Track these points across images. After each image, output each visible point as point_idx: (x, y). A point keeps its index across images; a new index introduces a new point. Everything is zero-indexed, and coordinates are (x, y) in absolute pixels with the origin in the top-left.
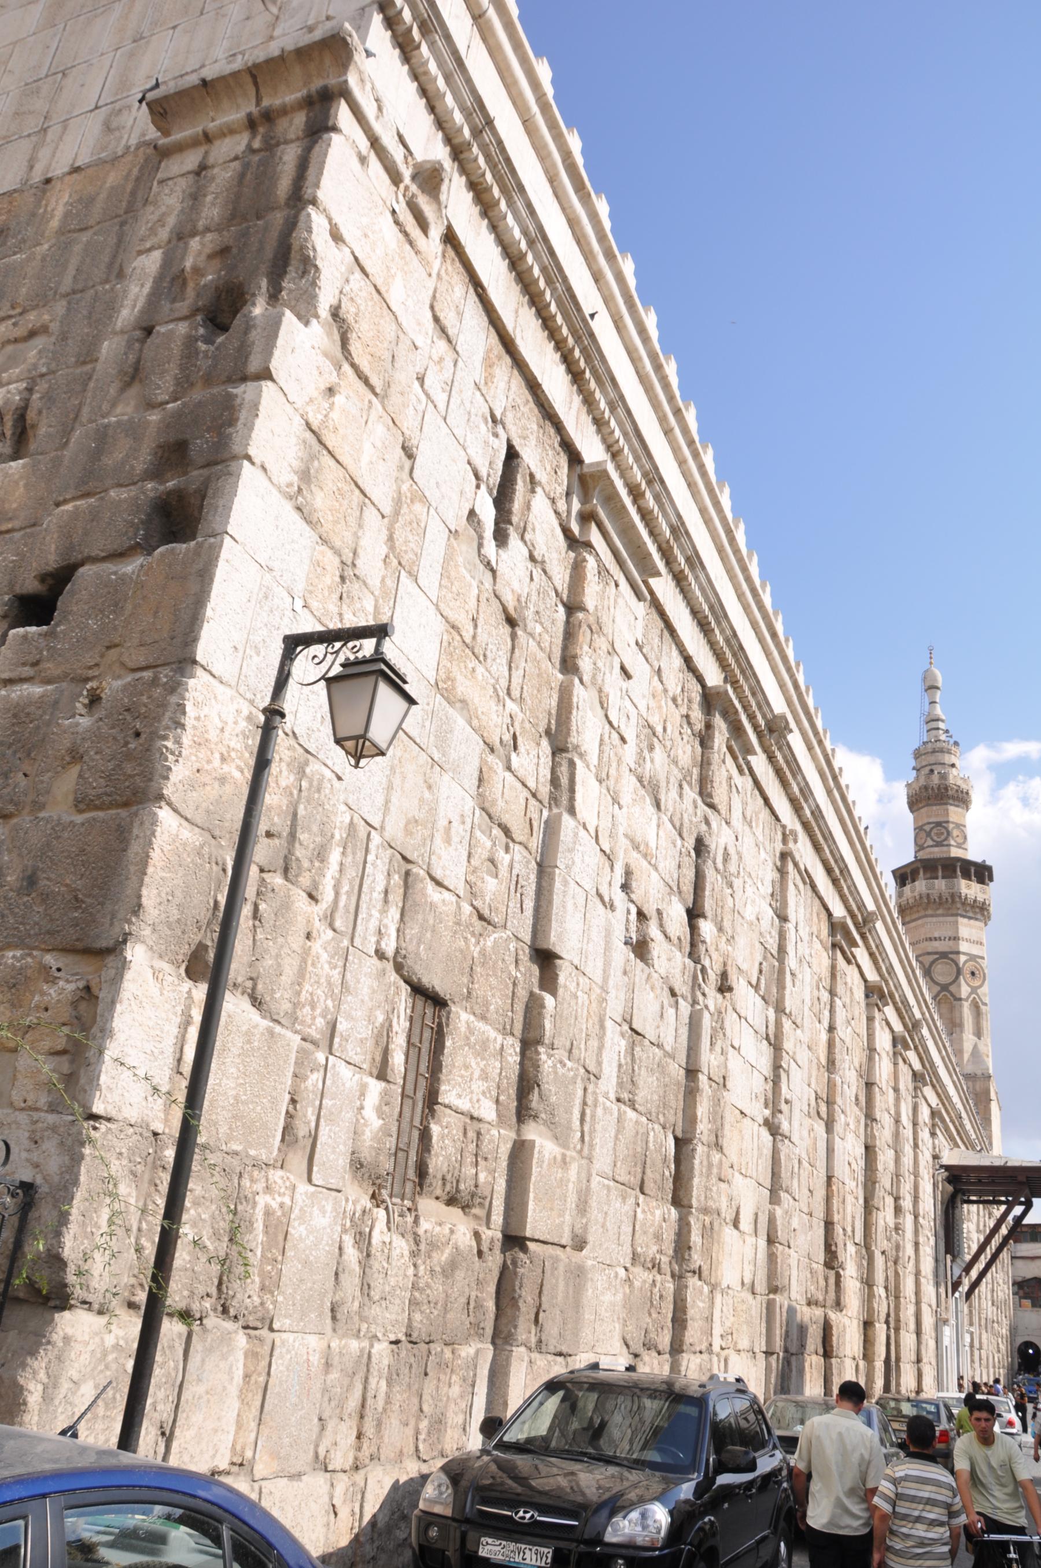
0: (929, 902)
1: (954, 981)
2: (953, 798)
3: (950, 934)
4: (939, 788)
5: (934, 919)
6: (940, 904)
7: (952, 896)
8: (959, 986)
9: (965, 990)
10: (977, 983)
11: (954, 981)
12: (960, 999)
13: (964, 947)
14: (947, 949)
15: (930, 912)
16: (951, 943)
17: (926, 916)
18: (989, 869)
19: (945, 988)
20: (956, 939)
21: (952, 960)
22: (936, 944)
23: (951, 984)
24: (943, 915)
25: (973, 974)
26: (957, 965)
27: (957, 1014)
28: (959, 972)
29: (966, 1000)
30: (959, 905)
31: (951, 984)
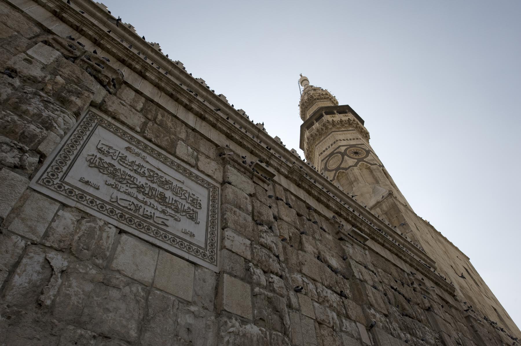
0: (314, 139)
2: (318, 99)
4: (308, 99)
5: (321, 144)
6: (321, 134)
7: (324, 125)
8: (346, 161)
10: (360, 157)
14: (333, 150)
15: (317, 143)
17: (316, 146)
18: (347, 107)
21: (337, 153)
22: (324, 154)
23: (341, 164)
24: (324, 138)
27: (351, 176)
29: (356, 165)
30: (330, 127)
31: (341, 164)
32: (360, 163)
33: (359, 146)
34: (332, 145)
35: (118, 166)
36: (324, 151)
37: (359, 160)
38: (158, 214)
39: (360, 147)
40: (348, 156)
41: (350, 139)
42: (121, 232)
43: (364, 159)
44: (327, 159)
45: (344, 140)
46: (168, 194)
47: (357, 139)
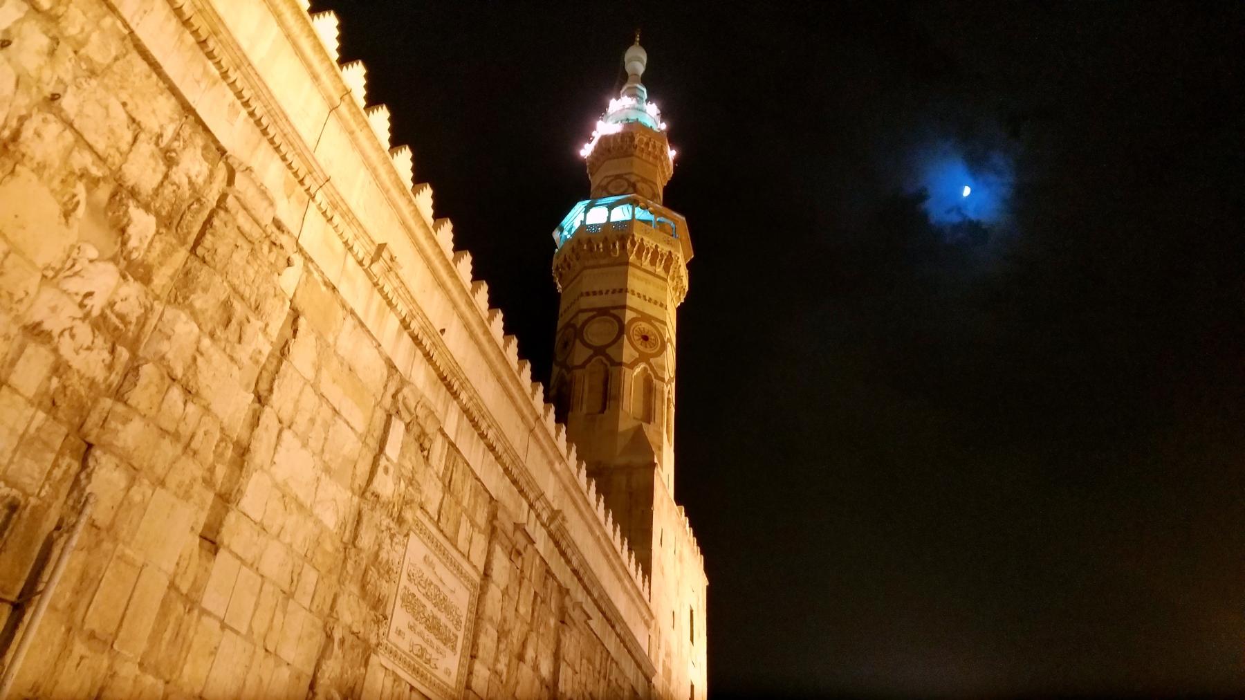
1: (614, 342)
3: (617, 286)
5: (596, 271)
8: (621, 347)
9: (628, 353)
10: (648, 351)
11: (614, 342)
12: (621, 364)
13: (631, 301)
16: (616, 296)
19: (600, 351)
20: (623, 291)
21: (615, 316)
23: (608, 346)
25: (645, 338)
26: (620, 321)
28: (622, 330)
31: (608, 346)
32: (642, 366)
33: (657, 324)
34: (614, 292)
35: (418, 595)
36: (594, 293)
37: (644, 358)
38: (435, 655)
39: (656, 328)
40: (629, 339)
41: (650, 300)
42: (412, 688)
43: (652, 360)
44: (591, 314)
45: (639, 296)
46: (443, 618)
47: (661, 305)
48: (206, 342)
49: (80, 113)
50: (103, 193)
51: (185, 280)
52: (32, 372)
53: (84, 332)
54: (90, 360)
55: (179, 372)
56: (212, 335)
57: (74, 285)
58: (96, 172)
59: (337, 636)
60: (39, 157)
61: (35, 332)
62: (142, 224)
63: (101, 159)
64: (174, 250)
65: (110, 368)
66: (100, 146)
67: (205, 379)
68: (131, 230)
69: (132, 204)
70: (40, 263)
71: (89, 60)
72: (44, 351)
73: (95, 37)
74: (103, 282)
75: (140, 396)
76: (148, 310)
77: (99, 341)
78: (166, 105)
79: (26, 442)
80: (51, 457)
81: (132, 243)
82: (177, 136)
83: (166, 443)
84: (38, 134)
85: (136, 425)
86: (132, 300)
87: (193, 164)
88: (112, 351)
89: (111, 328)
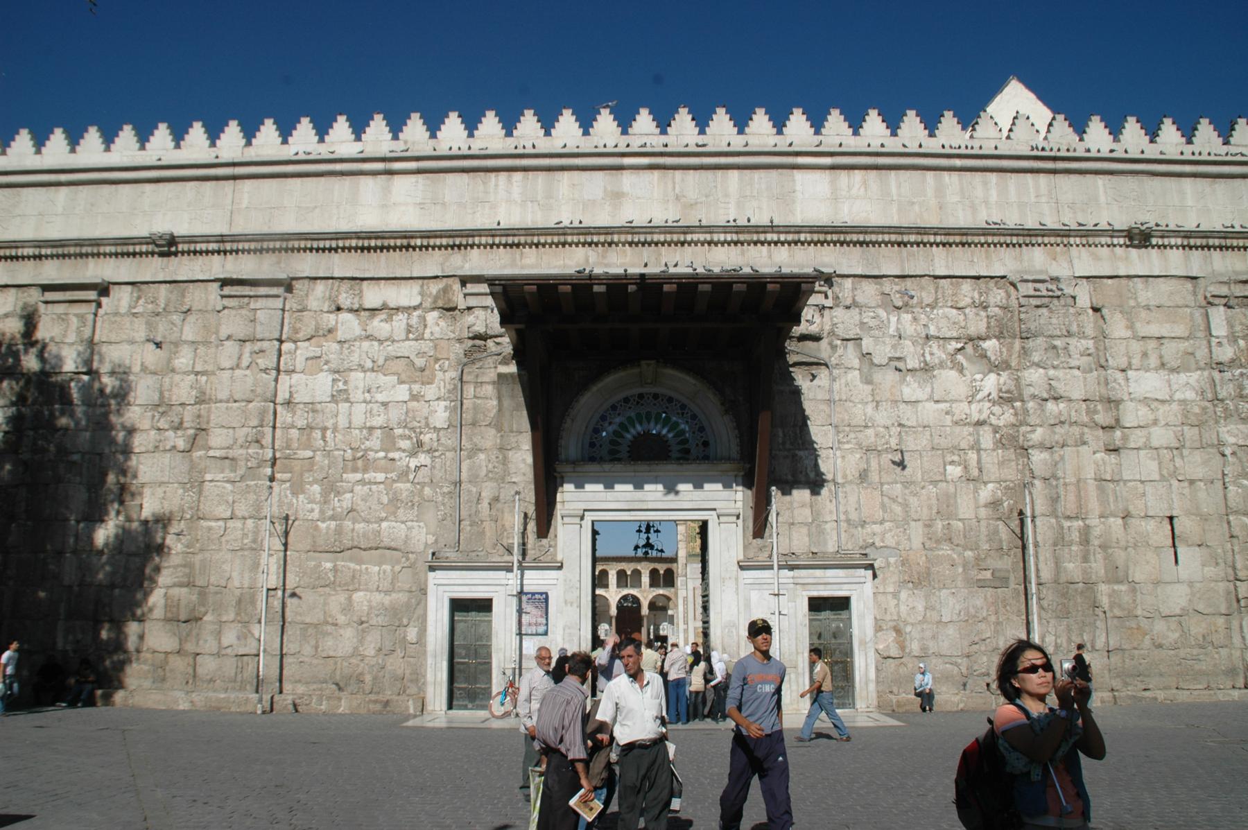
48: (1051, 372)
49: (939, 329)
50: (969, 349)
51: (1025, 352)
52: (987, 439)
53: (996, 409)
54: (1006, 417)
55: (1045, 395)
56: (1054, 367)
57: (979, 397)
58: (959, 346)
59: (1228, 451)
60: (937, 361)
61: (980, 423)
62: (990, 345)
63: (957, 339)
64: (1012, 344)
65: (1016, 414)
66: (955, 335)
67: (1061, 388)
68: (989, 354)
69: (981, 343)
70: (963, 397)
71: (928, 305)
72: (986, 428)
73: (924, 294)
74: (991, 383)
75: (1033, 419)
76: (1018, 380)
77: (1005, 408)
78: (966, 286)
79: (1001, 464)
80: (1013, 463)
81: (993, 358)
82: (981, 294)
83: (1058, 429)
84: (932, 354)
85: (1039, 430)
86: (1009, 381)
87: (997, 296)
88: (1013, 407)
89: (1006, 399)
